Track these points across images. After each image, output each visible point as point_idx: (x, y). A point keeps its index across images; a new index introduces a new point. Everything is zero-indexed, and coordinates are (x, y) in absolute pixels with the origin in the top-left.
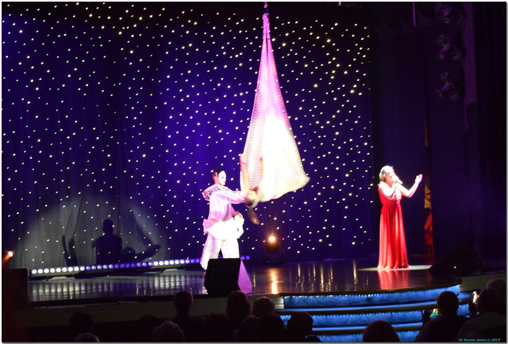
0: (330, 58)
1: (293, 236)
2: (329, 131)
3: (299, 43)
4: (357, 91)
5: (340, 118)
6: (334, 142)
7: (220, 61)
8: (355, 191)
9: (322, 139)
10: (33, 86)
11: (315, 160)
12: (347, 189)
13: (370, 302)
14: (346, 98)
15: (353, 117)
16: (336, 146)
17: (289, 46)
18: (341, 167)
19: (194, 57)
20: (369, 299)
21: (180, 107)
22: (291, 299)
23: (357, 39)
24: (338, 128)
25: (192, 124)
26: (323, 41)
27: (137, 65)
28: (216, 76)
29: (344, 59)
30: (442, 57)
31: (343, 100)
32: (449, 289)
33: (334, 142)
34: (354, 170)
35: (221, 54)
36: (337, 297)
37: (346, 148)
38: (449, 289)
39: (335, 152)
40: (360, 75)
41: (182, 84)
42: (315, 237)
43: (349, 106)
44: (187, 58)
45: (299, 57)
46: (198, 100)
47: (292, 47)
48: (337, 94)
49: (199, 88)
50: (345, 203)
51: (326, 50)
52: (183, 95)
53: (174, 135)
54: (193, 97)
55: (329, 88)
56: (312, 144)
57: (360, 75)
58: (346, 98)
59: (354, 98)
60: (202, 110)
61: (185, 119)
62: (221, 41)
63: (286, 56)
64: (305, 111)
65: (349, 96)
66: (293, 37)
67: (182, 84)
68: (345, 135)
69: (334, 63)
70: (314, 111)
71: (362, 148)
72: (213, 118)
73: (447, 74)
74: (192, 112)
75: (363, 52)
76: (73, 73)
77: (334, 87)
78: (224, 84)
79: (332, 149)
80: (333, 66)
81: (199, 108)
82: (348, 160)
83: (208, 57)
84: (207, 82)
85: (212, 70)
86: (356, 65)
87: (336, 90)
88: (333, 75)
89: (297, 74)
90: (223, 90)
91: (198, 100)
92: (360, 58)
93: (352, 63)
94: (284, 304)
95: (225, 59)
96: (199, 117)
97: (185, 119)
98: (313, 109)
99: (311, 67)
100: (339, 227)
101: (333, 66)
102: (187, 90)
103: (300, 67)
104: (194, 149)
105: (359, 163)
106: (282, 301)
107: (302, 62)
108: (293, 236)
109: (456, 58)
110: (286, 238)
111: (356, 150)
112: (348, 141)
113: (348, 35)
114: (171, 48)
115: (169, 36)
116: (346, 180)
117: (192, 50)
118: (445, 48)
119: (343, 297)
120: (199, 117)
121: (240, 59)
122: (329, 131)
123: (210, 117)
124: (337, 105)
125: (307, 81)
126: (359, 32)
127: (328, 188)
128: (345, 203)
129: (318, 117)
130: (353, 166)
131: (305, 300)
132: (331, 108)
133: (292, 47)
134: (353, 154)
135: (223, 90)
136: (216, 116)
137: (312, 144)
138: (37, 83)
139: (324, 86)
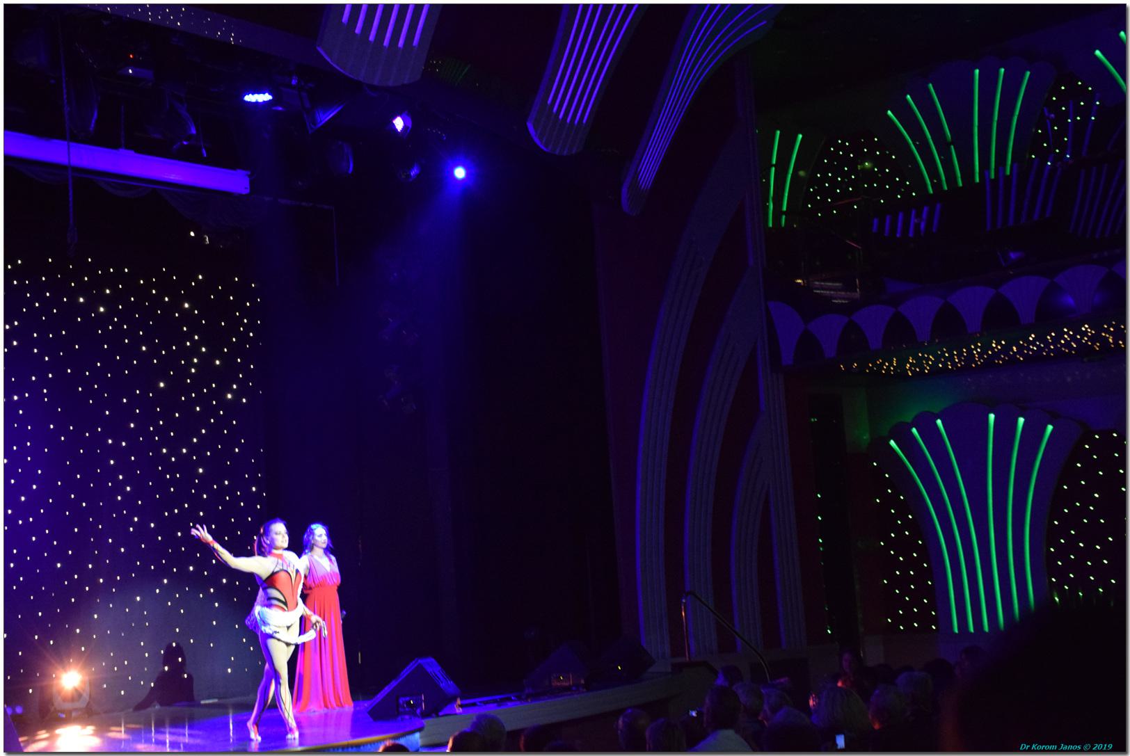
2: (186, 466)
3: (130, 309)
9: (173, 481)
14: (218, 408)
15: (231, 441)
17: (111, 311)
23: (239, 305)
29: (214, 339)
31: (209, 411)
37: (217, 497)
40: (243, 367)
45: (131, 333)
47: (118, 313)
48: (201, 400)
55: (187, 390)
57: (243, 367)
58: (218, 408)
63: (105, 330)
64: (142, 429)
65: (223, 403)
66: (117, 297)
68: (216, 471)
69: (196, 345)
70: (158, 429)
71: (247, 496)
75: (248, 328)
79: (190, 499)
80: (194, 350)
86: (237, 350)
87: (199, 393)
88: (194, 366)
89: (126, 363)
92: (243, 338)
98: (156, 426)
99: (154, 351)
101: (194, 350)
103: (133, 350)
107: (137, 341)
111: (236, 500)
112: (221, 485)
113: (222, 296)
122: (186, 466)
124: (201, 420)
125: (146, 376)
129: (165, 441)
132: (190, 424)
133: (118, 313)
134: (232, 508)
139: (177, 386)
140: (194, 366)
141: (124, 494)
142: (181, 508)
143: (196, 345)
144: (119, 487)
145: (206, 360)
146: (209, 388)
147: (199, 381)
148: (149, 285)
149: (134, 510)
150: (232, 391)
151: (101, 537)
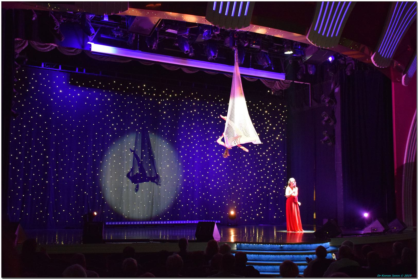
0: (266, 121)
1: (243, 211)
2: (264, 158)
4: (280, 138)
5: (270, 151)
6: (267, 164)
7: (210, 119)
8: (276, 190)
9: (261, 162)
10: (113, 127)
11: (257, 173)
12: (273, 188)
13: (282, 249)
14: (274, 141)
15: (277, 151)
16: (268, 166)
18: (270, 177)
19: (196, 116)
20: (281, 247)
21: (188, 142)
22: (240, 245)
23: (281, 112)
24: (269, 157)
25: (194, 151)
26: (263, 112)
27: (167, 119)
28: (207, 127)
29: (274, 121)
30: (324, 123)
32: (324, 245)
33: (267, 164)
34: (277, 179)
35: (210, 116)
36: (265, 245)
37: (273, 167)
38: (324, 245)
39: (267, 169)
40: (281, 130)
41: (189, 130)
42: (255, 213)
43: (275, 146)
44: (193, 117)
46: (197, 139)
49: (198, 133)
50: (271, 196)
51: (264, 117)
53: (184, 156)
54: (195, 137)
56: (255, 164)
57: (281, 130)
59: (278, 142)
60: (199, 144)
61: (190, 148)
62: (211, 109)
65: (275, 140)
67: (189, 130)
68: (273, 160)
69: (268, 123)
71: (281, 167)
72: (205, 149)
73: (326, 132)
74: (194, 145)
75: (283, 119)
76: (134, 122)
77: (268, 135)
78: (211, 131)
79: (265, 167)
81: (197, 143)
82: (274, 173)
83: (204, 117)
84: (203, 130)
85: (205, 123)
87: (269, 137)
90: (211, 134)
91: (197, 139)
92: (282, 121)
93: (278, 124)
95: (213, 119)
96: (197, 148)
97: (190, 148)
100: (267, 208)
101: (268, 125)
102: (192, 133)
104: (194, 163)
105: (279, 175)
106: (236, 246)
108: (243, 211)
109: (331, 124)
110: (239, 212)
111: (278, 168)
113: (276, 109)
114: (184, 112)
115: (184, 105)
116: (272, 184)
117: (195, 113)
118: (326, 118)
120: (197, 148)
122: (264, 158)
123: (203, 148)
126: (282, 108)
127: (263, 187)
128: (271, 196)
130: (276, 177)
131: (248, 246)
134: (277, 171)
135: (211, 134)
136: (206, 147)
137: (255, 164)
138: (115, 126)
141: (247, 165)
142: (263, 170)
143: (268, 123)
144: (246, 163)
146: (271, 136)
147: (269, 134)
148: (256, 106)
149: (250, 170)
150: (278, 137)
151: (241, 176)
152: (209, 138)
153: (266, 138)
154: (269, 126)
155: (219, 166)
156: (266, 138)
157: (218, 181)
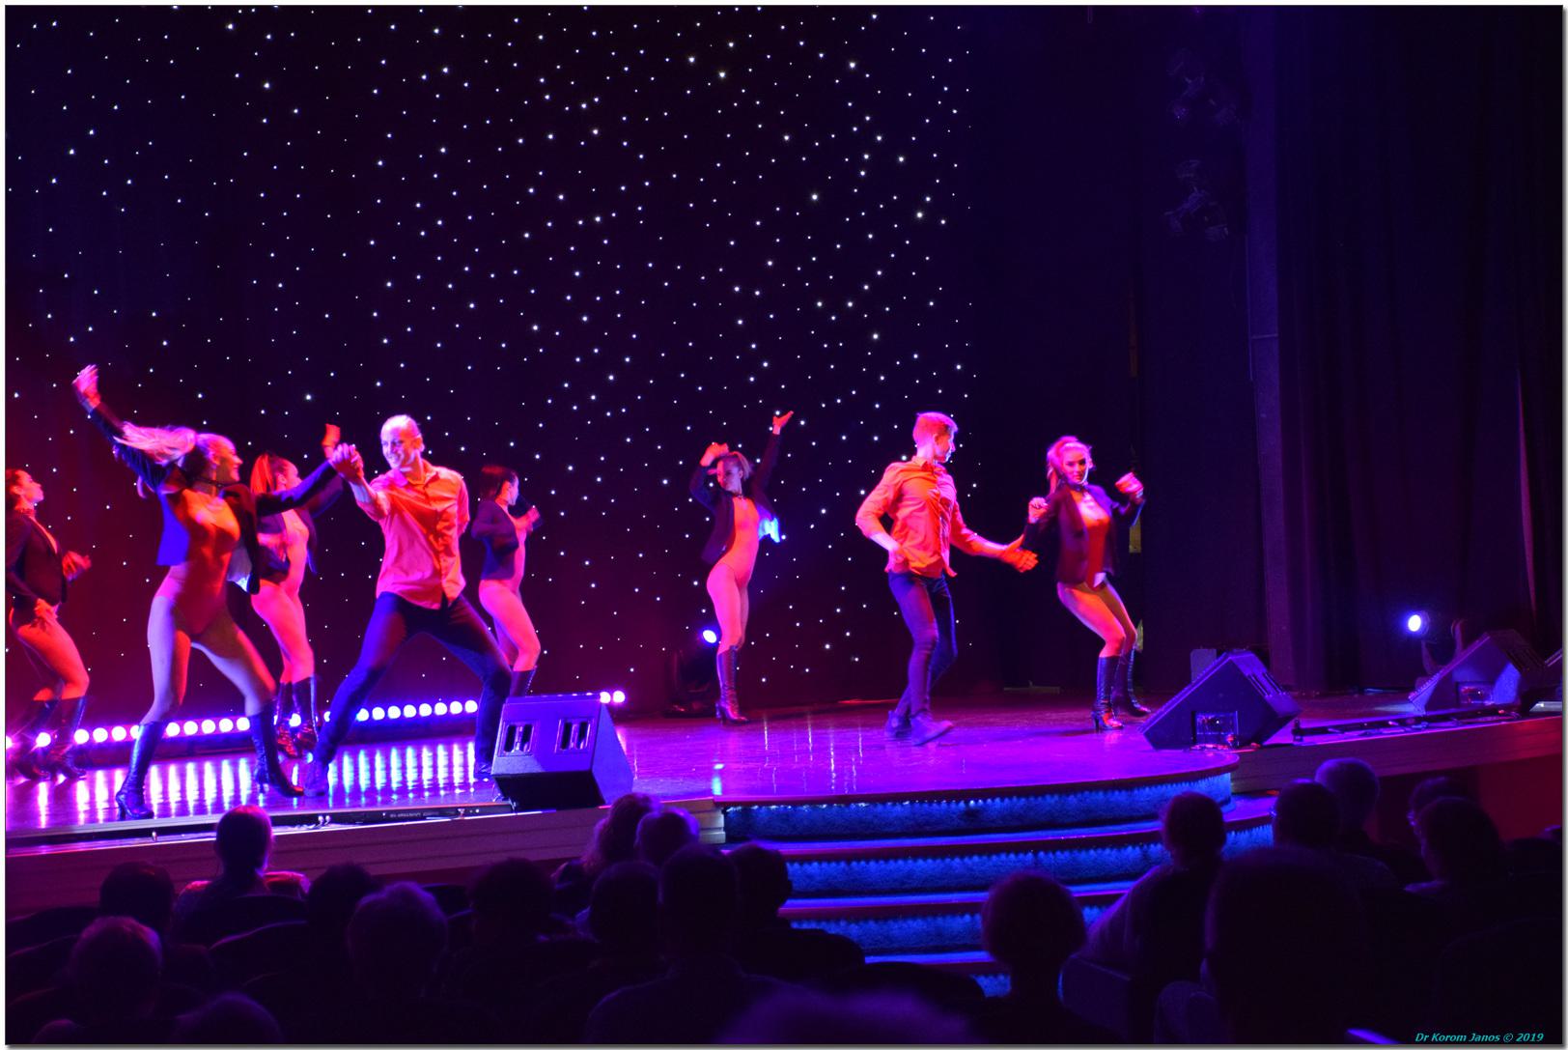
13: (974, 822)
20: (971, 814)
32: (1202, 786)
36: (880, 807)
38: (1202, 786)
52: (425, 219)
65: (911, 228)
69: (868, 131)
78: (547, 189)
88: (864, 165)
94: (726, 829)
98: (807, 264)
99: (801, 143)
101: (865, 140)
106: (721, 821)
119: (898, 808)
121: (594, 116)
131: (785, 817)
140: (864, 165)
142: (847, 397)
143: (868, 131)
144: (751, 363)
145: (883, 154)
150: (924, 207)
152: (538, 230)
153: (855, 217)
154: (873, 148)
155: (602, 388)
156: (855, 217)
157: (599, 469)
